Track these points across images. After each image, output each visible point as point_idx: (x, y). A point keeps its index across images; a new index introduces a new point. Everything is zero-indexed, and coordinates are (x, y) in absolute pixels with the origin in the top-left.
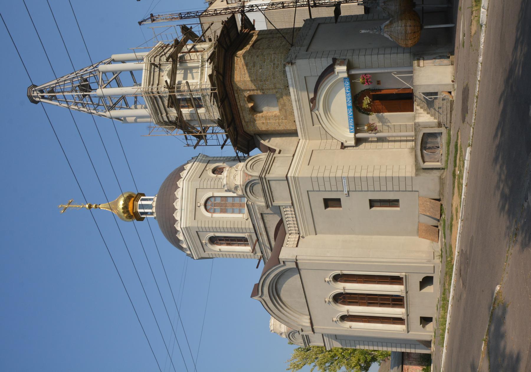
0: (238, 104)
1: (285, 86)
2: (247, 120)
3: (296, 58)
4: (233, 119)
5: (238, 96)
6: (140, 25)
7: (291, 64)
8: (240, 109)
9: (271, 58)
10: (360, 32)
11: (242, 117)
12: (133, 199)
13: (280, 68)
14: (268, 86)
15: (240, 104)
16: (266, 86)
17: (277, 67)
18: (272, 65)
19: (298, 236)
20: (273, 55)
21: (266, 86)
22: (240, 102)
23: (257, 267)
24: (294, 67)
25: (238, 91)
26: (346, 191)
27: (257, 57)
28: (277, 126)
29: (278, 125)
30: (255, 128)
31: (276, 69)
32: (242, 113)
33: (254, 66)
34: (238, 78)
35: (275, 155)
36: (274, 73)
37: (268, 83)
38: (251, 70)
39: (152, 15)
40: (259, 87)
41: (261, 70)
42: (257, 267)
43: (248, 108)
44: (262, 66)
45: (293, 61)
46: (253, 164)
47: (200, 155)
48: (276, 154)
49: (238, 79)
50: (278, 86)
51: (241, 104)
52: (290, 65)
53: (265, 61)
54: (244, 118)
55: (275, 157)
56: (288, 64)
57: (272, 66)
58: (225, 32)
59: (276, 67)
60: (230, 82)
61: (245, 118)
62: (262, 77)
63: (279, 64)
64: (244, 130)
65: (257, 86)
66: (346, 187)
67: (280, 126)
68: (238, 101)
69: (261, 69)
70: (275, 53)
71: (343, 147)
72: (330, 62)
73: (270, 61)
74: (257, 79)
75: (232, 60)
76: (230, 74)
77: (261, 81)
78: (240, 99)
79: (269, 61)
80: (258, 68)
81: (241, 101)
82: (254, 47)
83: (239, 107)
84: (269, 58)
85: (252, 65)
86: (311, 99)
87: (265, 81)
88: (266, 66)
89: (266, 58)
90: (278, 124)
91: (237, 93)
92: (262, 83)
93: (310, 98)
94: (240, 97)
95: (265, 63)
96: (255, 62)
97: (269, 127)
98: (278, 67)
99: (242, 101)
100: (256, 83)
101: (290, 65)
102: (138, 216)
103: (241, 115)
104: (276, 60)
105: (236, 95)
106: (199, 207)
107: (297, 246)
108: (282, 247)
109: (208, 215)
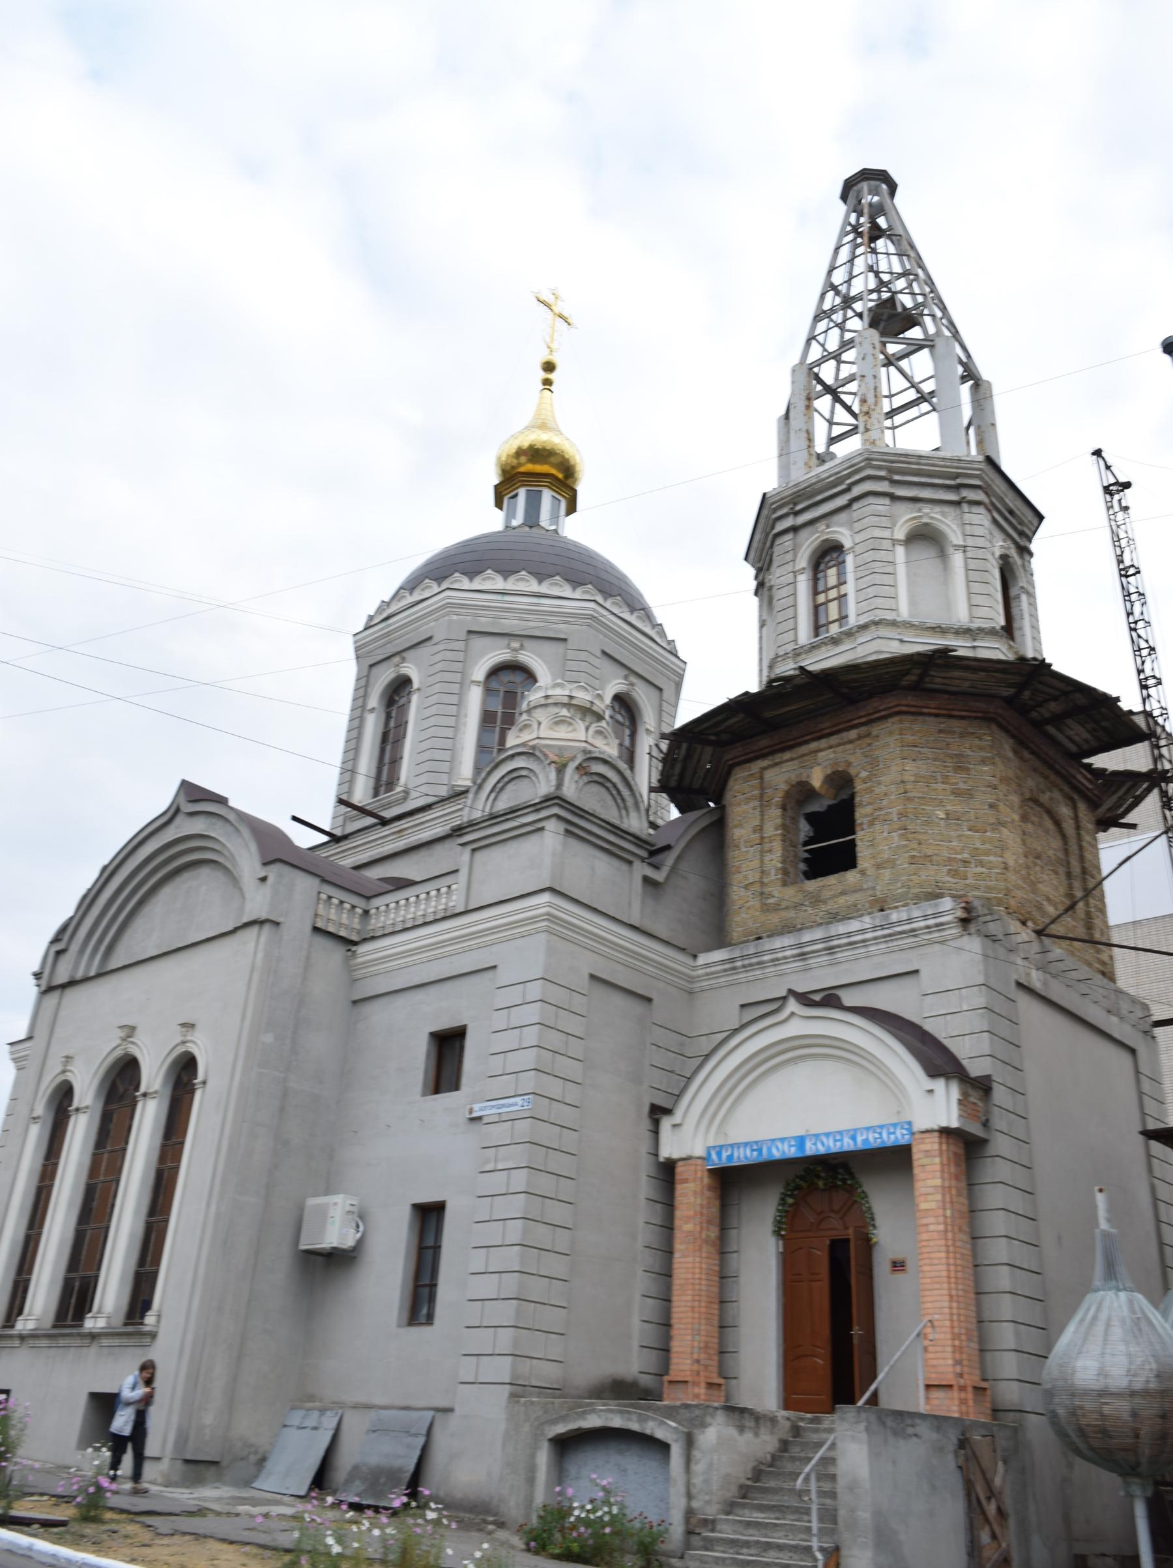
0: (823, 743)
1: (884, 900)
2: (768, 775)
3: (987, 936)
4: (773, 726)
5: (851, 742)
6: (1093, 454)
7: (964, 915)
8: (804, 749)
9: (987, 853)
10: (1097, 1188)
11: (778, 757)
12: (560, 476)
13: (949, 882)
14: (885, 838)
15: (821, 750)
16: (885, 834)
17: (954, 873)
18: (960, 854)
19: (355, 938)
20: (1000, 859)
21: (885, 834)
22: (831, 747)
23: (295, 819)
24: (954, 931)
25: (868, 740)
26: (481, 1110)
27: (991, 806)
28: (746, 878)
29: (747, 882)
30: (739, 804)
31: (945, 869)
32: (792, 759)
33: (957, 793)
34: (912, 738)
35: (637, 864)
36: (931, 861)
37: (896, 839)
38: (943, 783)
39: (1127, 485)
40: (880, 809)
41: (942, 816)
42: (295, 819)
43: (808, 776)
44: (958, 819)
45: (973, 927)
46: (609, 785)
47: (682, 665)
48: (642, 869)
49: (907, 737)
50: (886, 874)
51: (823, 753)
52: (960, 914)
53: (977, 831)
54: (776, 765)
55: (630, 863)
56: (963, 905)
57: (959, 857)
58: (1080, 699)
59: (956, 871)
60: (897, 709)
61: (776, 770)
62: (918, 818)
63: (968, 882)
64: (737, 769)
65: (884, 803)
66: (494, 1111)
67: (746, 887)
68: (833, 740)
69: (947, 814)
70: (1006, 868)
71: (658, 1113)
72: (976, 1069)
73: (977, 849)
74: (909, 799)
75: (977, 718)
76: (926, 710)
77: (901, 815)
78: (840, 749)
79: (978, 845)
80: (949, 808)
81: (834, 752)
82: (1031, 804)
83: (813, 745)
84: (988, 846)
85: (962, 786)
86: (838, 998)
87: (900, 829)
88: (959, 836)
89: (988, 834)
90: (751, 881)
91: (860, 738)
92: (895, 819)
93: (841, 993)
94: (848, 746)
95: (969, 833)
96: (971, 796)
97: (744, 849)
98: (953, 876)
99: (832, 756)
100: (893, 797)
101: (960, 914)
102: (506, 489)
103: (787, 755)
104: (980, 870)
105: (853, 734)
106: (509, 644)
107: (316, 929)
108: (317, 881)
109: (479, 673)
